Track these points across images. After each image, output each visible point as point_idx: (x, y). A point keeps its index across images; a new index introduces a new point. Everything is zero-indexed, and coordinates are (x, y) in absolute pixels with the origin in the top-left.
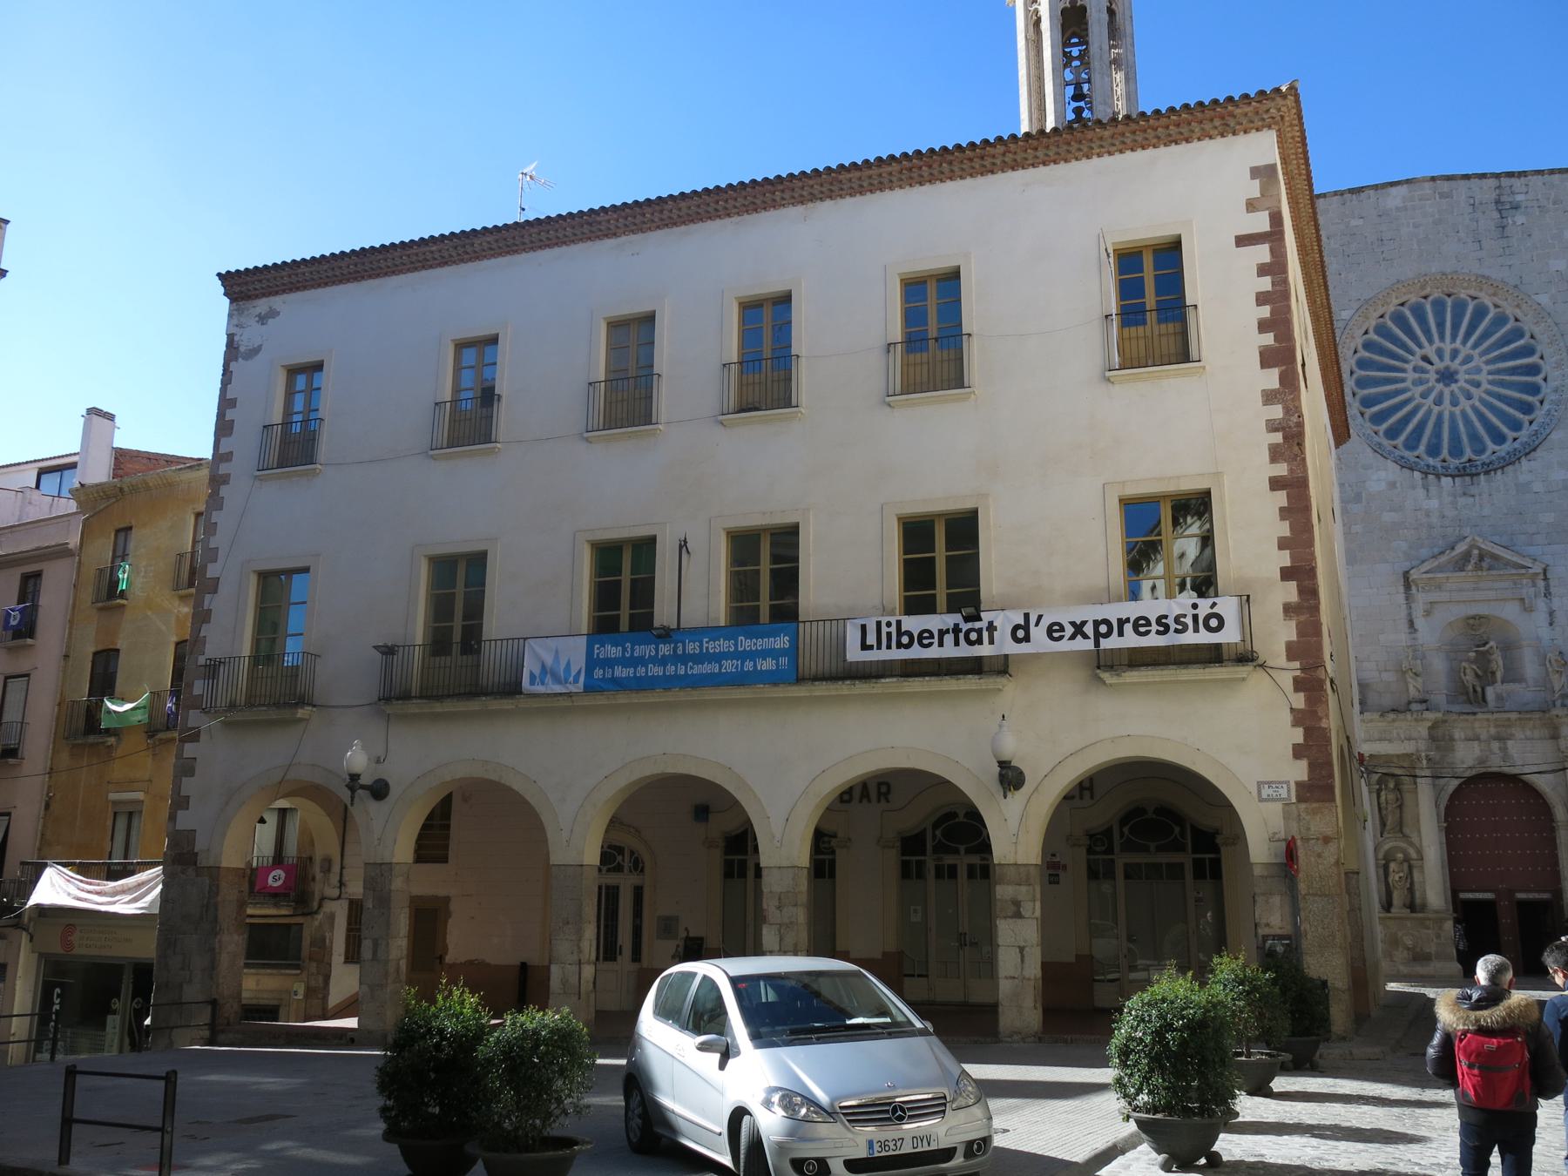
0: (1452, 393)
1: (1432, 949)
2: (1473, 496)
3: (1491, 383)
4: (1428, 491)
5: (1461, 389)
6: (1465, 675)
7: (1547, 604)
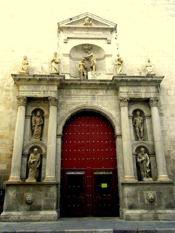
1: (42, 203)
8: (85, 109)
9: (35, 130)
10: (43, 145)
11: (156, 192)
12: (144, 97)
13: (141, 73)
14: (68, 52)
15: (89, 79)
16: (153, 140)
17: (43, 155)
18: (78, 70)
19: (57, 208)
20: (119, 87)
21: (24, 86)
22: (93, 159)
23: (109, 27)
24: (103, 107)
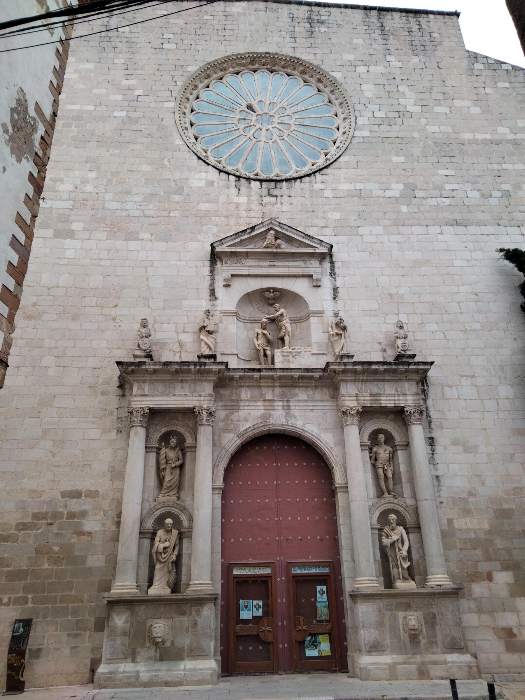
2: (276, 196)
4: (239, 190)
6: (257, 341)
8: (270, 430)
9: (167, 478)
10: (184, 509)
11: (424, 614)
12: (393, 405)
14: (232, 307)
15: (278, 365)
16: (414, 496)
17: (184, 532)
18: (255, 345)
19: (215, 655)
20: (339, 383)
21: (142, 384)
23: (317, 251)
24: (307, 425)
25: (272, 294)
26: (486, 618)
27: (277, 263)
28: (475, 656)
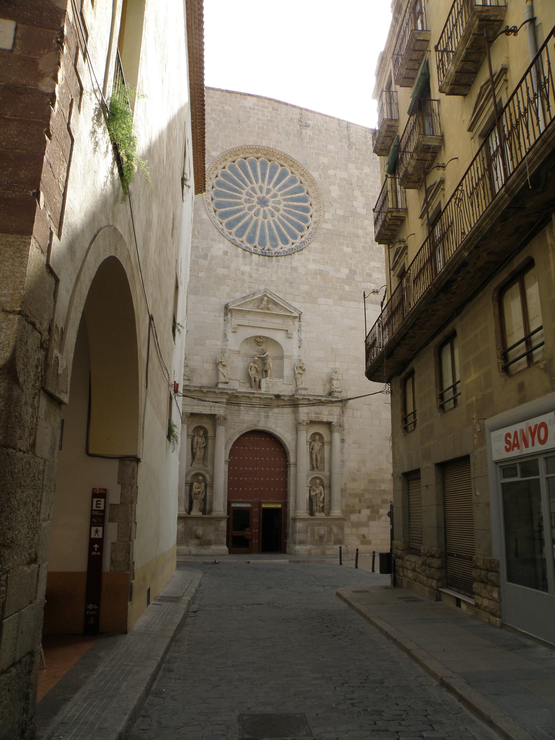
0: (264, 211)
1: (212, 537)
3: (285, 211)
5: (269, 209)
7: (298, 335)
9: (198, 453)
10: (207, 472)
13: (325, 385)
16: (330, 471)
22: (261, 490)
24: (277, 428)
25: (261, 340)
26: (354, 530)
27: (267, 319)
28: (346, 546)
